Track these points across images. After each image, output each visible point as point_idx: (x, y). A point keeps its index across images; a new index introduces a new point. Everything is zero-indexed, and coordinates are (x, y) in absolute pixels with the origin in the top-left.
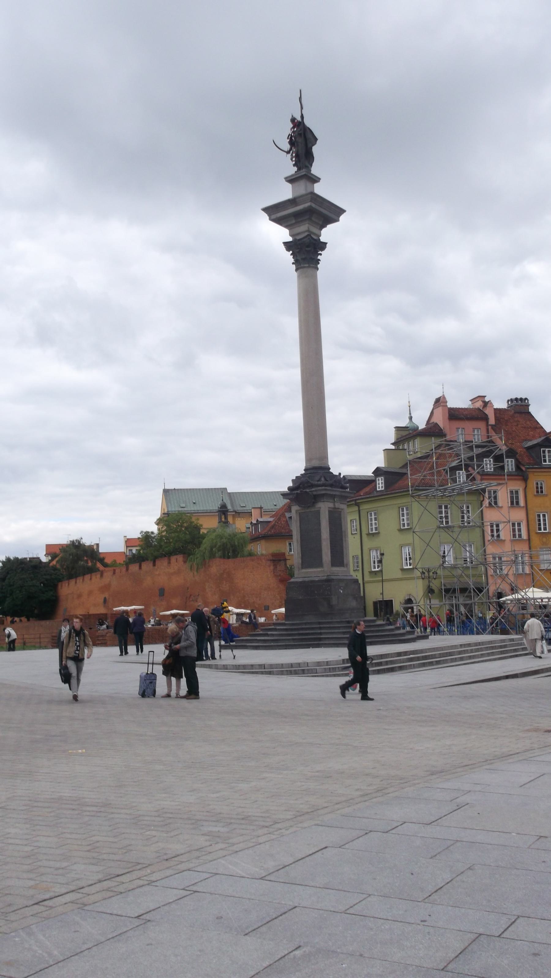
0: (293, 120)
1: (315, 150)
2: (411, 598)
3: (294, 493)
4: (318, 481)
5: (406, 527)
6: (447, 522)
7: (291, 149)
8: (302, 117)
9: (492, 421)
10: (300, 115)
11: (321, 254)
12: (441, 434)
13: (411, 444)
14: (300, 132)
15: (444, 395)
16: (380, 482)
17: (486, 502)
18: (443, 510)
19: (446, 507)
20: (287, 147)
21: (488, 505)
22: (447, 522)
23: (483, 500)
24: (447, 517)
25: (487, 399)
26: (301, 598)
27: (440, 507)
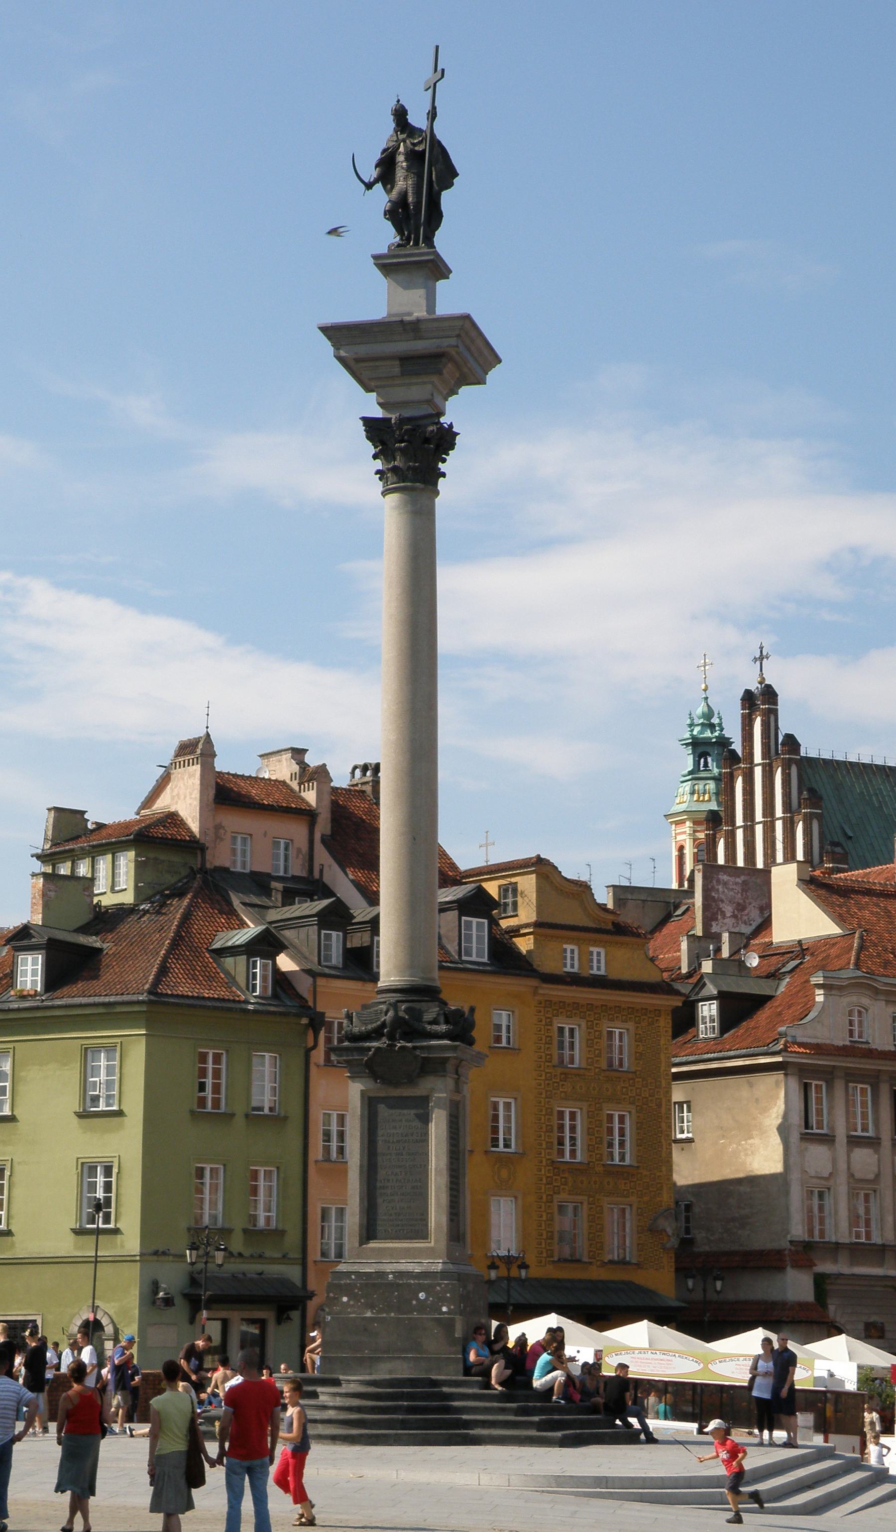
0: (400, 114)
1: (447, 198)
2: (98, 1317)
3: (369, 1049)
4: (430, 1023)
5: (102, 1107)
6: (216, 1103)
7: (376, 181)
8: (433, 115)
9: (323, 826)
10: (428, 107)
11: (444, 461)
12: (195, 845)
13: (104, 864)
14: (419, 148)
15: (208, 735)
16: (29, 968)
17: (318, 1055)
18: (210, 1066)
19: (217, 1059)
20: (370, 172)
21: (322, 1061)
22: (216, 1103)
23: (315, 1045)
24: (216, 1088)
25: (312, 760)
26: (369, 1314)
27: (203, 1058)
